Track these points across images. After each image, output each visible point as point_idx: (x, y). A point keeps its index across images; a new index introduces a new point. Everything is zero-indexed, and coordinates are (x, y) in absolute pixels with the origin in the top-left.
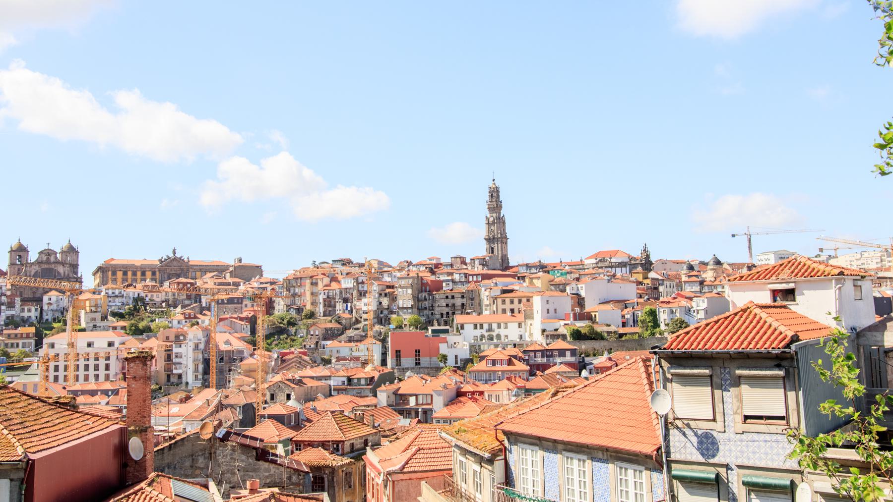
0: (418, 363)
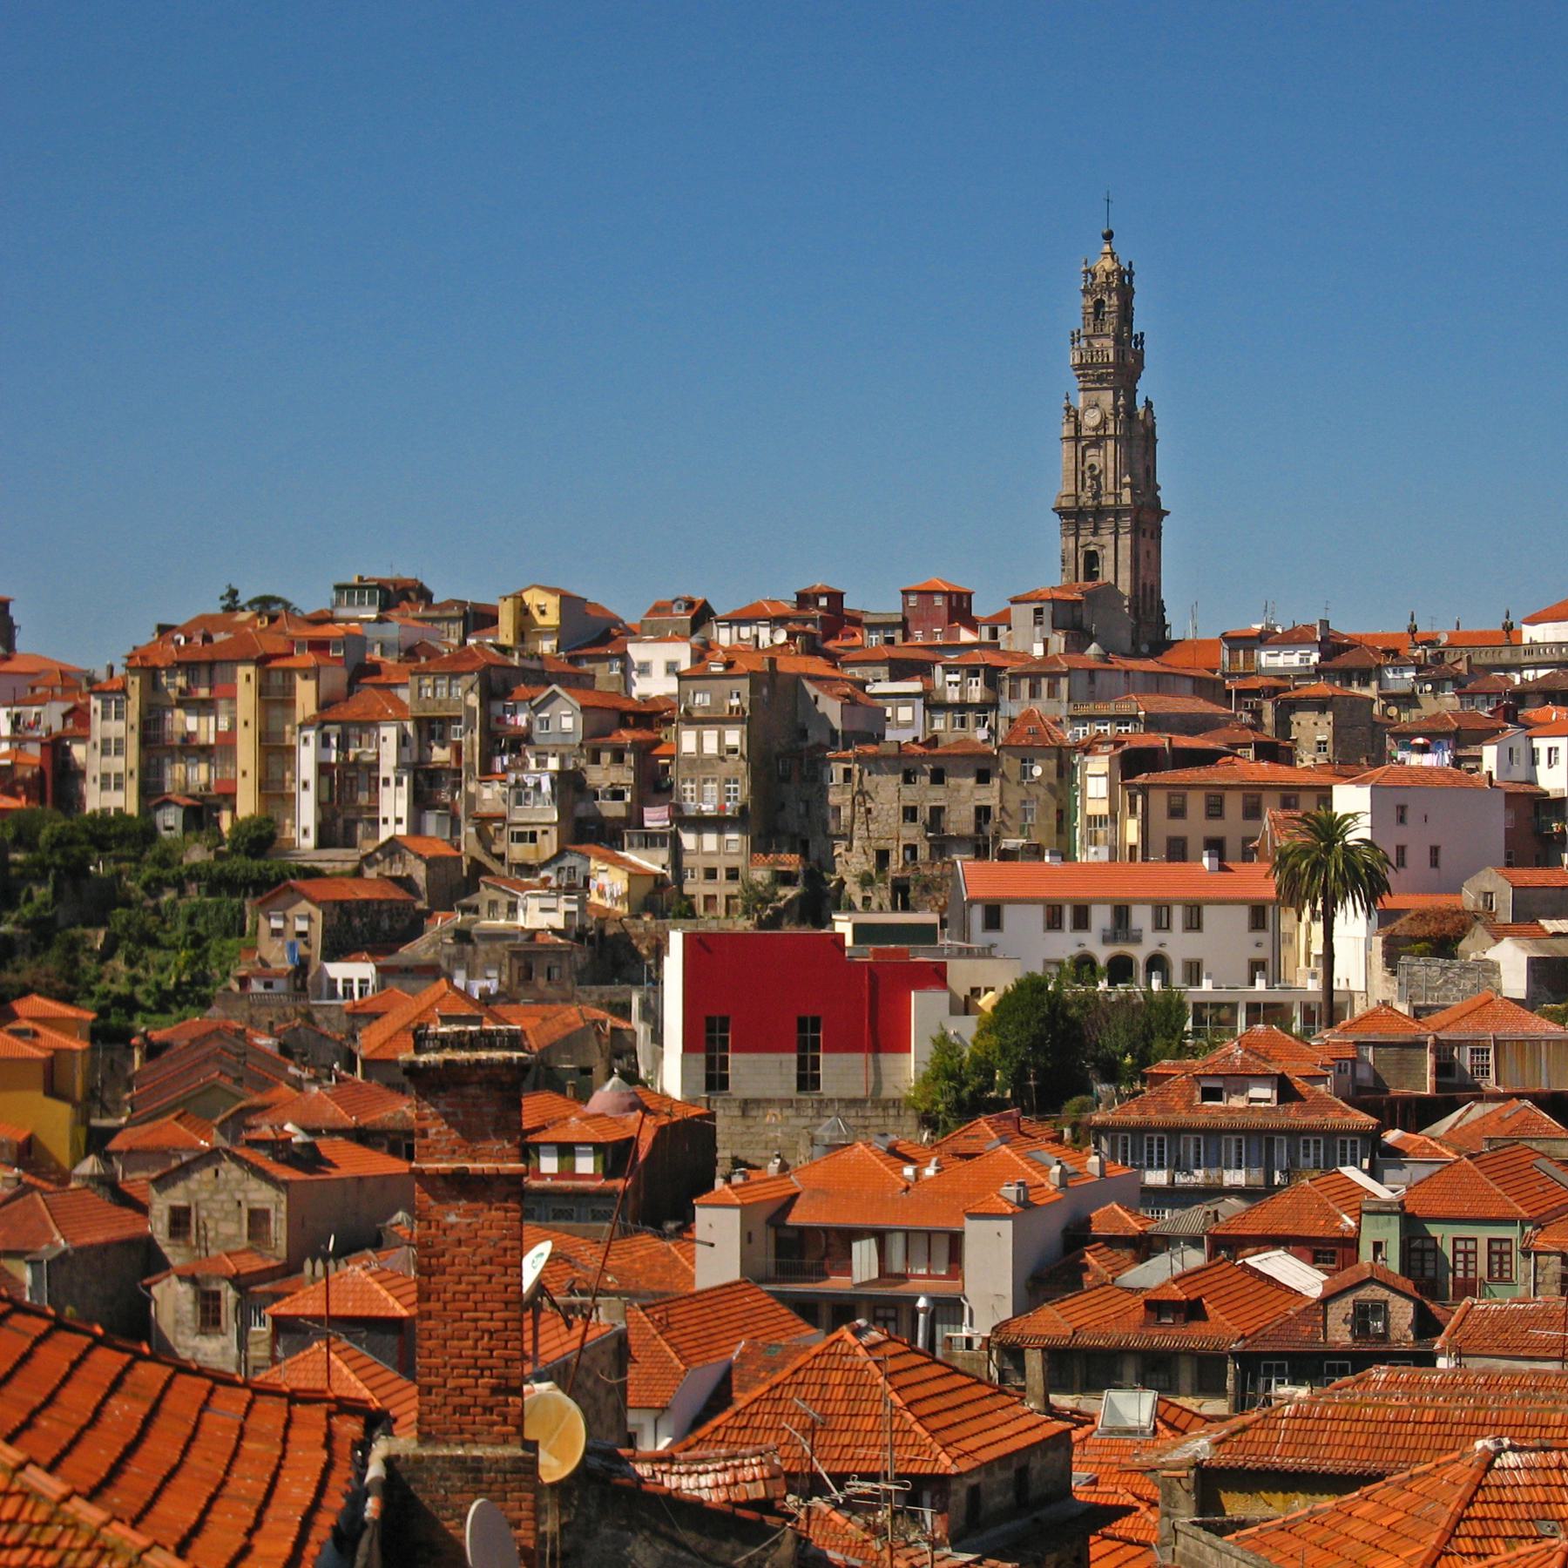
0: (808, 1080)
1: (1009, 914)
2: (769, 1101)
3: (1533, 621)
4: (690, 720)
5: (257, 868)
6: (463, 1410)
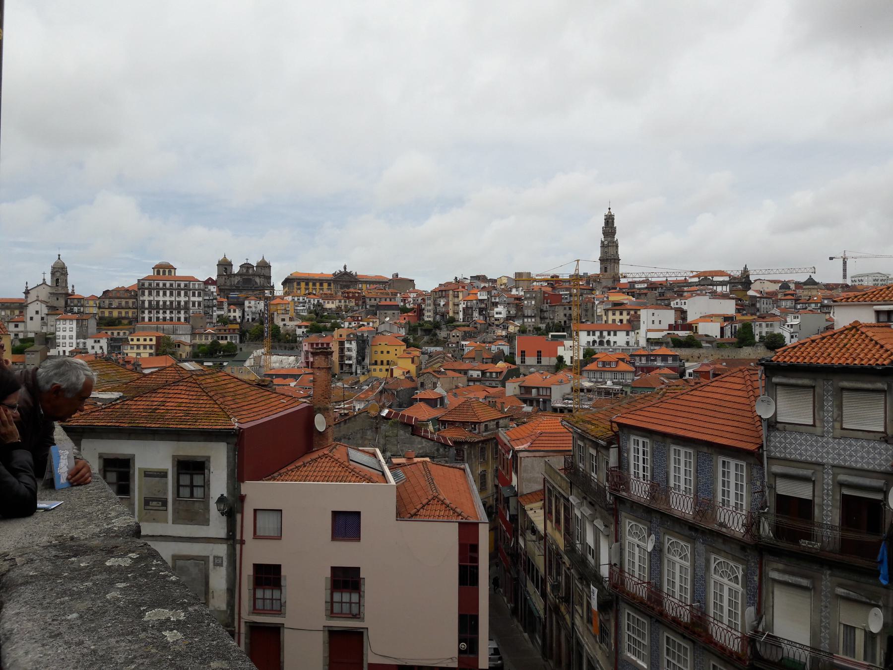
0: (539, 362)
4: (526, 299)
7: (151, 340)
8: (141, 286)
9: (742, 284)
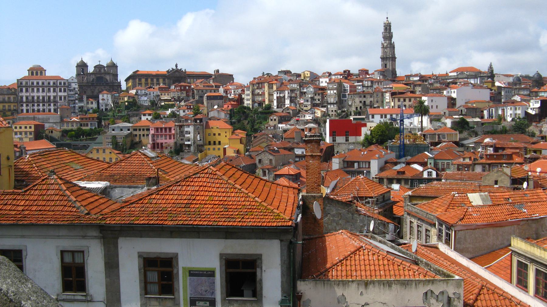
0: (347, 140)
1: (375, 116)
2: (342, 143)
3: (450, 72)
4: (329, 89)
5: (268, 111)
6: (312, 189)
7: (30, 127)
8: (21, 84)
9: (488, 77)
